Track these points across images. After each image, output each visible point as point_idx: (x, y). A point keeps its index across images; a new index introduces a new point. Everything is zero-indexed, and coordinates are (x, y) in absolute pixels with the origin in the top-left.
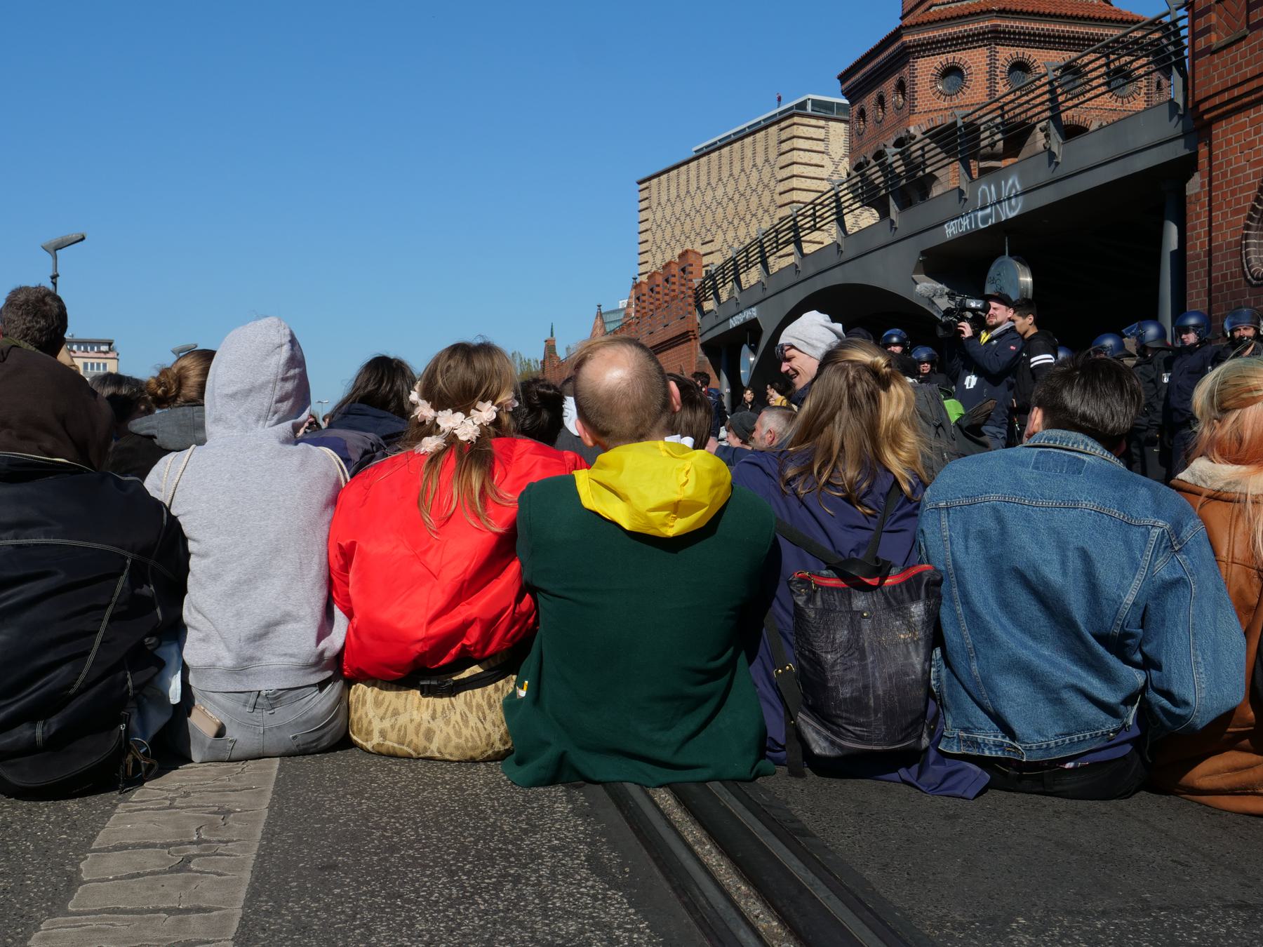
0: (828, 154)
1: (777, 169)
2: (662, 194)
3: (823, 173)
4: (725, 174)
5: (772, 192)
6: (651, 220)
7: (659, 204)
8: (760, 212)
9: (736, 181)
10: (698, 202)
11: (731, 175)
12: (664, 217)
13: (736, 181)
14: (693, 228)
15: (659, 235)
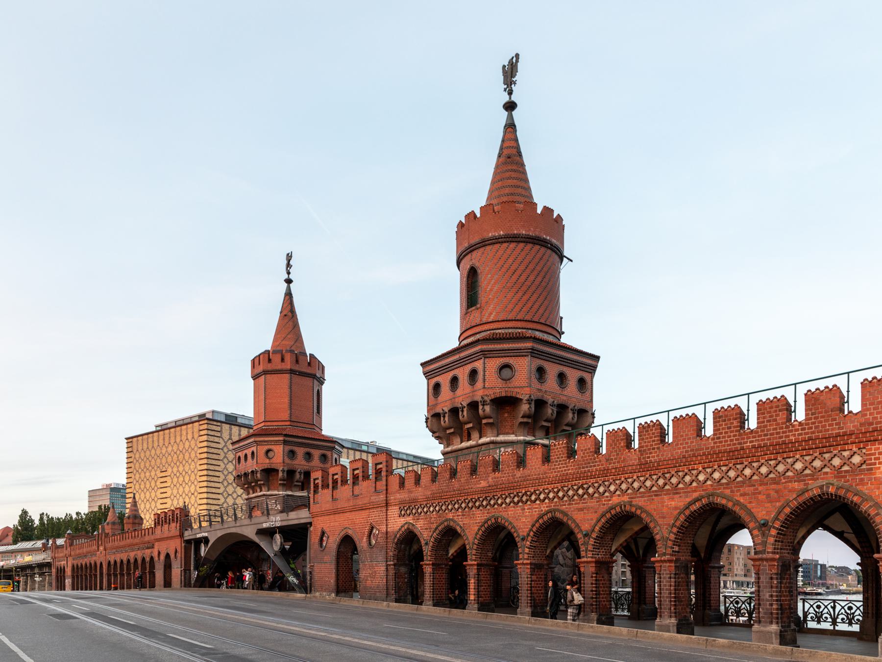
0: (222, 438)
1: (198, 442)
2: (139, 446)
3: (220, 446)
4: (172, 441)
5: (196, 453)
6: (133, 458)
7: (137, 450)
8: (190, 461)
9: (178, 445)
10: (158, 452)
11: (175, 442)
12: (140, 457)
13: (178, 445)
14: (156, 464)
15: (137, 465)
